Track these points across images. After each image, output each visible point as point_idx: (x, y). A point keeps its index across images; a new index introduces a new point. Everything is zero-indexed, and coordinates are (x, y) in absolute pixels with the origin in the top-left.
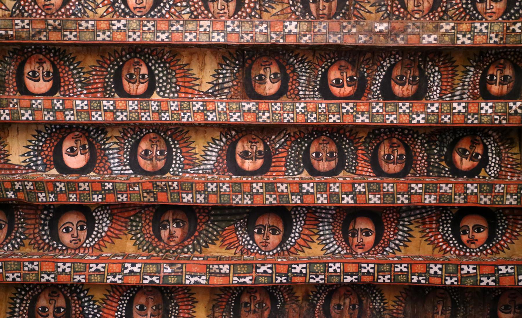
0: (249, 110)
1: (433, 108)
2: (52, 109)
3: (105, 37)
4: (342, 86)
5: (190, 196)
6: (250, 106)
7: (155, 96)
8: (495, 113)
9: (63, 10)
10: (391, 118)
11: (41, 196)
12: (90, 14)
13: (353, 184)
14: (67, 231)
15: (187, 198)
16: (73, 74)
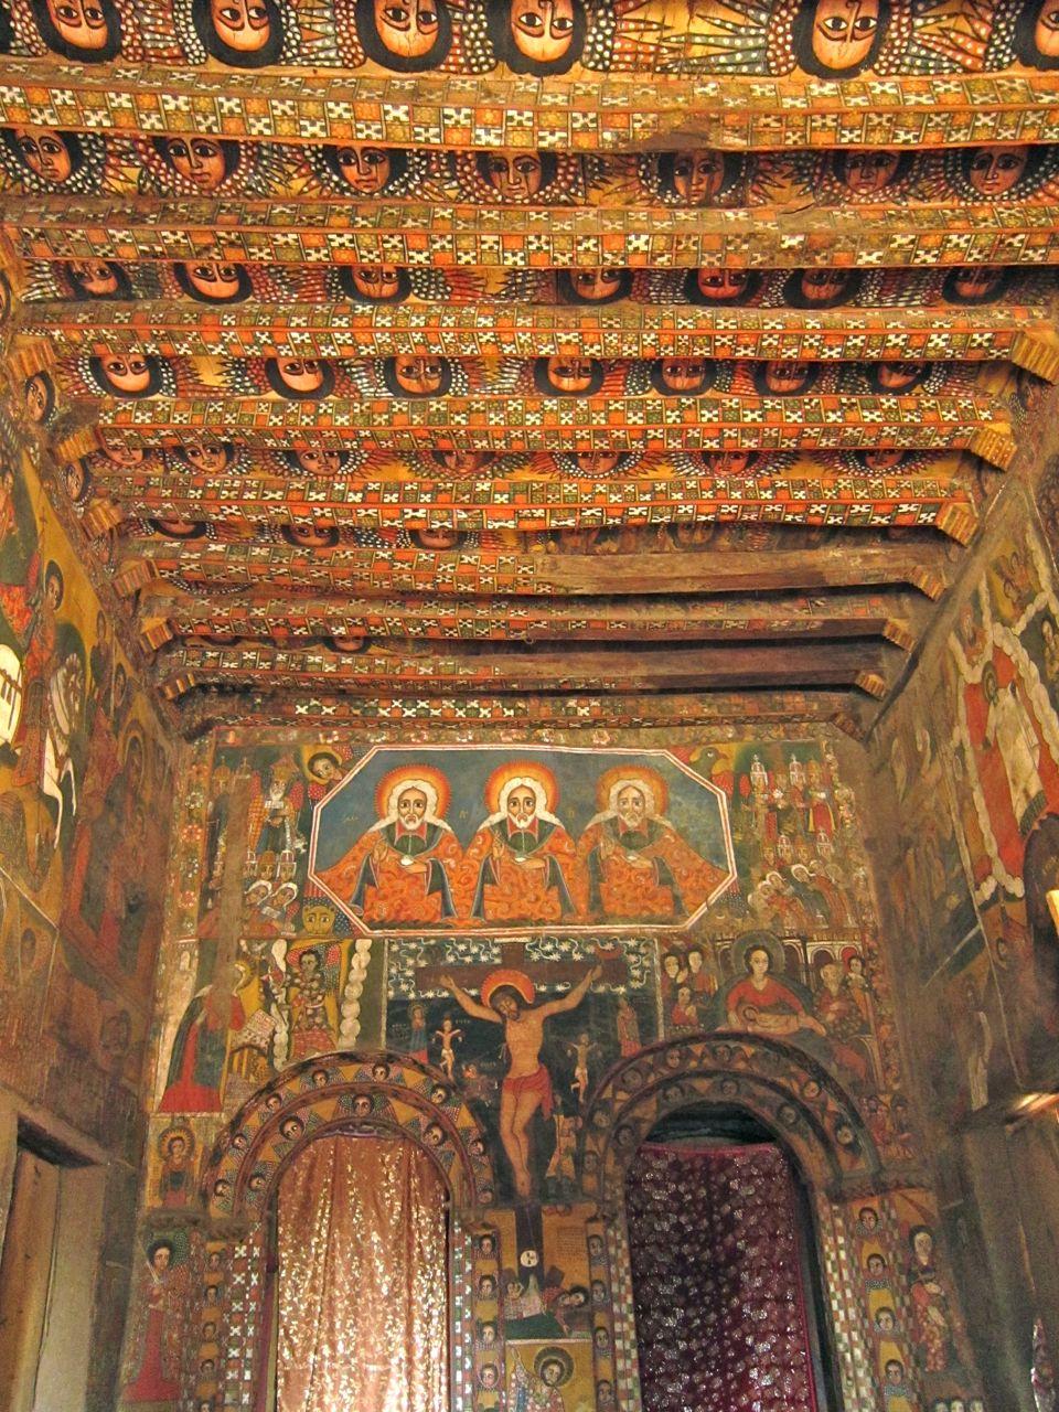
0: (568, 342)
1: (858, 341)
2: (257, 343)
3: (321, 256)
4: (722, 285)
5: (485, 443)
6: (570, 337)
7: (412, 299)
8: (948, 347)
9: (228, 182)
10: (790, 353)
11: (270, 442)
12: (280, 188)
13: (721, 430)
14: (311, 456)
15: (481, 445)
16: (270, 274)
